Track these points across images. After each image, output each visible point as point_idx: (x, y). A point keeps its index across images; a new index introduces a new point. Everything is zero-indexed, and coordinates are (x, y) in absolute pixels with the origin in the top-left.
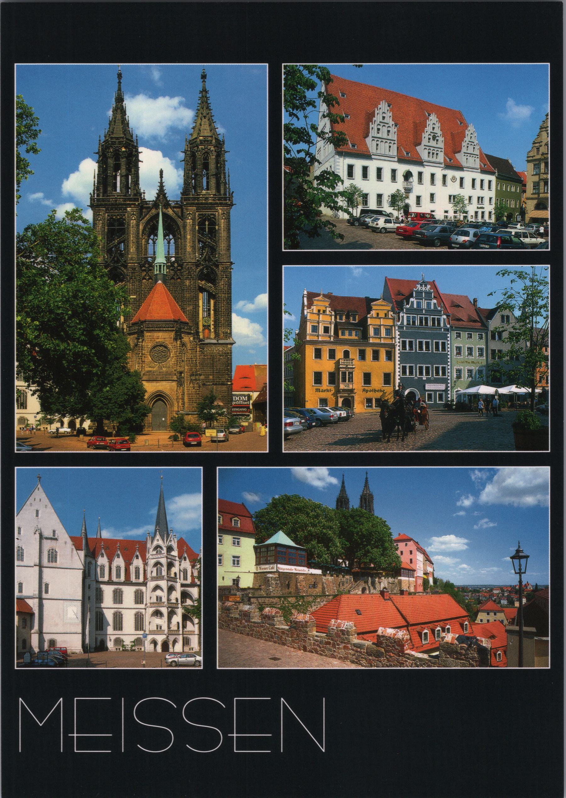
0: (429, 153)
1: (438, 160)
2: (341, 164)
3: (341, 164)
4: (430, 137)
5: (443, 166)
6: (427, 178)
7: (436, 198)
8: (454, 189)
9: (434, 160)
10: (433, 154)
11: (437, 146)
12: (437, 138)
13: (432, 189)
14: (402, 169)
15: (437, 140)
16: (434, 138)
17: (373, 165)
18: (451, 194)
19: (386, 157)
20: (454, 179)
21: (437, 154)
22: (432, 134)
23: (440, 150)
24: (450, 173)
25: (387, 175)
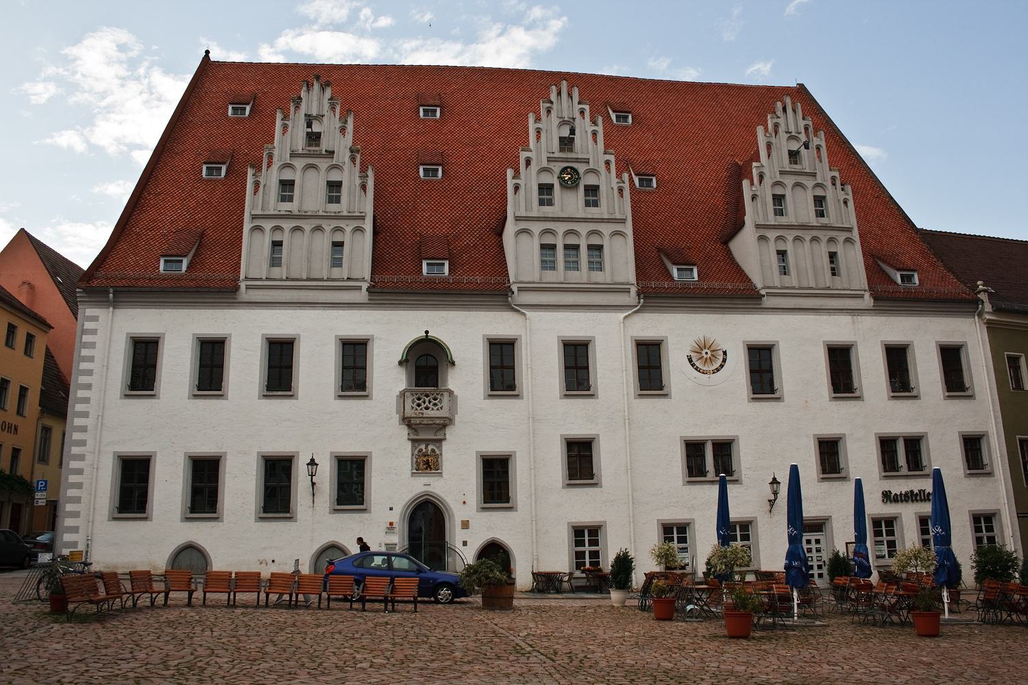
0: (548, 248)
1: (598, 277)
4: (546, 179)
5: (632, 298)
6: (540, 366)
7: (606, 460)
8: (707, 401)
9: (583, 275)
10: (572, 248)
12: (591, 180)
13: (577, 418)
14: (392, 332)
15: (592, 190)
16: (570, 179)
17: (245, 332)
18: (696, 433)
20: (707, 357)
22: (557, 167)
23: (606, 229)
24: (678, 330)
25: (317, 367)
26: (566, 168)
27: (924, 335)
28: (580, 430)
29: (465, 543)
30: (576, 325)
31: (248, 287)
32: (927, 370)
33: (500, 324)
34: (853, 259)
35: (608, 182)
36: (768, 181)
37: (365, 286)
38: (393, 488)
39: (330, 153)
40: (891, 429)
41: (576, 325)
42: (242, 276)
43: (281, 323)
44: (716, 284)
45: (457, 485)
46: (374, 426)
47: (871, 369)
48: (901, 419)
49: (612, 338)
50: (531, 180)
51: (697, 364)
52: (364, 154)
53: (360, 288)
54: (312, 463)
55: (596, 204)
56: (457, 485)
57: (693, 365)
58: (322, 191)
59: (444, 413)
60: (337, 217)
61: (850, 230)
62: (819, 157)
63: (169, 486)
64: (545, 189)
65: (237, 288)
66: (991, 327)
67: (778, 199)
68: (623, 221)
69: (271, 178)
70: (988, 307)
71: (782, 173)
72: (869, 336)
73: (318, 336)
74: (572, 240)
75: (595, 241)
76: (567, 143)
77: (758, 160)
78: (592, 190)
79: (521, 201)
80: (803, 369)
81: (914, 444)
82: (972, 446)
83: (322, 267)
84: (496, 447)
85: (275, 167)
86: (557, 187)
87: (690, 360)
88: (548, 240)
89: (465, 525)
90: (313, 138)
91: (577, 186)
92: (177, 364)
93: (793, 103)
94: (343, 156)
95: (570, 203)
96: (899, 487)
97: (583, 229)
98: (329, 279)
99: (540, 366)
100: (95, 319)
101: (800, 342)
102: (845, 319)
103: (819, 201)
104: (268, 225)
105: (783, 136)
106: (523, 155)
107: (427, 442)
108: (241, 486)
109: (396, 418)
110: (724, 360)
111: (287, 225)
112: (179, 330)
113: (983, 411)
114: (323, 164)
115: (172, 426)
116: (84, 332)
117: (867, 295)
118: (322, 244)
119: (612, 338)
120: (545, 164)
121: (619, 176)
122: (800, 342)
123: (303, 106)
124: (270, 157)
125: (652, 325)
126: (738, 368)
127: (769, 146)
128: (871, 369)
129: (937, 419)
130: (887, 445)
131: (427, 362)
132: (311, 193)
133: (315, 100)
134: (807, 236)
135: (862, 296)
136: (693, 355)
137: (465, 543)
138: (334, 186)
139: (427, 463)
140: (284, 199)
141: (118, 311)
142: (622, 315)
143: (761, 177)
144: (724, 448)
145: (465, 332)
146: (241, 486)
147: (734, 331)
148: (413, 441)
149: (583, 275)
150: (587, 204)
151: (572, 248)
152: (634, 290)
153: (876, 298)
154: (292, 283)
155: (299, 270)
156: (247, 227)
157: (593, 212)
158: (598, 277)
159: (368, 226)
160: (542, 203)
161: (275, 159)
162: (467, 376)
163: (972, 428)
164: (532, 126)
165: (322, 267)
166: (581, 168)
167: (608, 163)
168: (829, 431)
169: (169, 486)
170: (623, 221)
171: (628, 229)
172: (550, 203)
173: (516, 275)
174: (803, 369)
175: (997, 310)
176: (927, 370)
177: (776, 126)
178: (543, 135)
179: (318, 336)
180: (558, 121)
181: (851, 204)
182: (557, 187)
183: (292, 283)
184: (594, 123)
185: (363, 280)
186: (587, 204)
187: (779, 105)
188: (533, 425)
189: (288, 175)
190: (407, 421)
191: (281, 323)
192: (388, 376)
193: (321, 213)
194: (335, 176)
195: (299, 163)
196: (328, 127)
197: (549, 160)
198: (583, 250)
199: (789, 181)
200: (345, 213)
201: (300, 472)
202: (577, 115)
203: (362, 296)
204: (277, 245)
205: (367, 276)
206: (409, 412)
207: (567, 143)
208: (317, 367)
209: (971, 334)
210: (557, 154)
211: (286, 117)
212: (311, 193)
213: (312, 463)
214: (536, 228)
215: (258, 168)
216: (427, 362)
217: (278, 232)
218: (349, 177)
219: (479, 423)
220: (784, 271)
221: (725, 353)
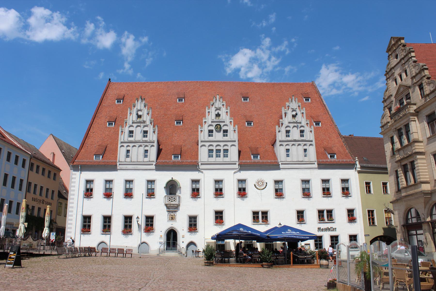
0: (211, 151)
1: (226, 159)
2: (77, 180)
3: (77, 180)
5: (237, 166)
6: (207, 189)
8: (260, 199)
10: (218, 151)
11: (225, 138)
12: (225, 128)
14: (162, 178)
15: (226, 131)
16: (218, 128)
17: (118, 178)
18: (256, 209)
19: (137, 166)
20: (260, 185)
21: (226, 151)
22: (214, 124)
23: (229, 144)
24: (252, 177)
25: (139, 189)
26: (217, 125)
27: (335, 176)
28: (219, 209)
29: (183, 242)
30: (218, 175)
31: (120, 164)
32: (336, 188)
33: (195, 175)
34: (312, 150)
35: (230, 128)
36: (284, 126)
37: (154, 163)
38: (162, 225)
39: (144, 122)
40: (321, 208)
41: (218, 175)
42: (118, 161)
43: (129, 175)
44: (265, 161)
45: (181, 225)
46: (157, 207)
47: (316, 188)
48: (325, 204)
49: (230, 179)
50: (206, 129)
51: (257, 187)
52: (154, 123)
53: (152, 164)
54: (138, 218)
55: (227, 136)
56: (181, 225)
57: (256, 187)
58: (141, 135)
59: (177, 203)
60: (146, 142)
61: (312, 141)
62: (303, 116)
63: (97, 224)
64: (211, 131)
65: (116, 165)
66: (359, 172)
67: (288, 132)
68: (235, 141)
69: (126, 130)
70: (358, 166)
71: (289, 123)
72: (316, 176)
73: (140, 179)
74: (218, 148)
75: (226, 148)
76: (218, 115)
77: (282, 119)
78: (226, 131)
79: (203, 136)
80: (292, 188)
81: (330, 212)
82: (350, 212)
83: (141, 158)
84: (193, 214)
85: (128, 126)
86: (214, 131)
87: (255, 185)
88: (211, 148)
89: (183, 237)
90: (139, 116)
91: (220, 130)
92: (99, 189)
93: (295, 99)
94: (148, 123)
95: (218, 136)
96: (323, 226)
97: (222, 144)
98: (144, 162)
99: (207, 189)
100: (75, 174)
101: (292, 179)
102: (308, 171)
103: (302, 132)
104: (125, 145)
105: (290, 110)
106: (204, 121)
107: (172, 212)
108: (117, 224)
109: (163, 204)
110: (266, 186)
111: (131, 145)
112: (99, 178)
113: (356, 201)
114: (142, 125)
115: (97, 207)
116: (73, 178)
117: (316, 163)
118: (142, 150)
119: (230, 179)
120: (210, 123)
121: (234, 126)
122: (292, 179)
123: (136, 107)
124: (126, 123)
125: (243, 175)
126: (271, 188)
127: (285, 113)
128: (316, 188)
129: (338, 204)
130: (321, 212)
131: (172, 188)
132: (138, 135)
133: (140, 105)
134: (297, 143)
135: (314, 164)
136: (256, 184)
137: (183, 242)
138: (145, 132)
139: (172, 218)
140: (130, 136)
141: (83, 173)
142: (233, 171)
143: (282, 124)
144: (265, 214)
145: (184, 178)
146: (117, 224)
147: (269, 176)
148: (168, 211)
149: (221, 159)
150: (224, 136)
151: (218, 151)
152: (237, 163)
153: (318, 164)
154: (132, 163)
155: (134, 159)
156: (119, 145)
157: (225, 138)
158: (226, 159)
159: (155, 144)
160: (209, 136)
161: (128, 124)
162: (185, 191)
163: (351, 207)
164: (207, 111)
165: (141, 158)
166: (222, 124)
167: (231, 122)
168: (300, 208)
169: (97, 224)
170: (235, 141)
171: (236, 143)
172: (212, 136)
173: (200, 160)
174: (292, 188)
175: (362, 167)
176: (336, 188)
177: (288, 106)
178: (210, 113)
179: (140, 179)
180: (215, 109)
181: (313, 132)
182: (214, 131)
183: (132, 163)
184: (227, 109)
185: (153, 161)
186: (224, 136)
187: (290, 99)
188: (204, 207)
189: (131, 129)
190: (166, 205)
191: (129, 175)
192: (160, 191)
193: (141, 141)
194: (146, 129)
195: (135, 125)
196: (144, 112)
197: (212, 122)
198: (222, 151)
199: (292, 125)
200: (149, 141)
201: (134, 221)
202: (221, 106)
203: (153, 167)
204: (128, 151)
205: (155, 161)
206: (167, 203)
207: (218, 115)
208: (139, 189)
209: (352, 175)
210: (215, 120)
211: (131, 109)
212: (138, 135)
213: (138, 218)
214: (207, 144)
215: (123, 127)
216: (172, 188)
217: (128, 147)
218: (150, 129)
219: (187, 206)
220: (288, 155)
221: (266, 183)
